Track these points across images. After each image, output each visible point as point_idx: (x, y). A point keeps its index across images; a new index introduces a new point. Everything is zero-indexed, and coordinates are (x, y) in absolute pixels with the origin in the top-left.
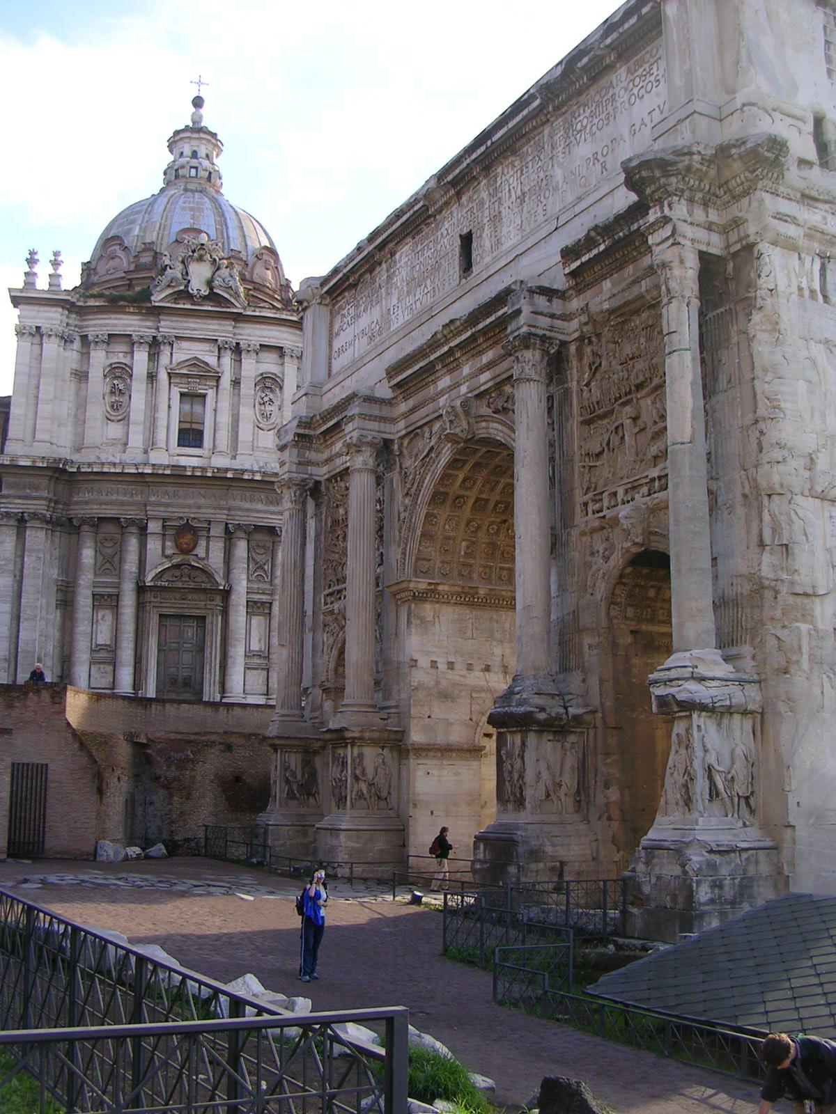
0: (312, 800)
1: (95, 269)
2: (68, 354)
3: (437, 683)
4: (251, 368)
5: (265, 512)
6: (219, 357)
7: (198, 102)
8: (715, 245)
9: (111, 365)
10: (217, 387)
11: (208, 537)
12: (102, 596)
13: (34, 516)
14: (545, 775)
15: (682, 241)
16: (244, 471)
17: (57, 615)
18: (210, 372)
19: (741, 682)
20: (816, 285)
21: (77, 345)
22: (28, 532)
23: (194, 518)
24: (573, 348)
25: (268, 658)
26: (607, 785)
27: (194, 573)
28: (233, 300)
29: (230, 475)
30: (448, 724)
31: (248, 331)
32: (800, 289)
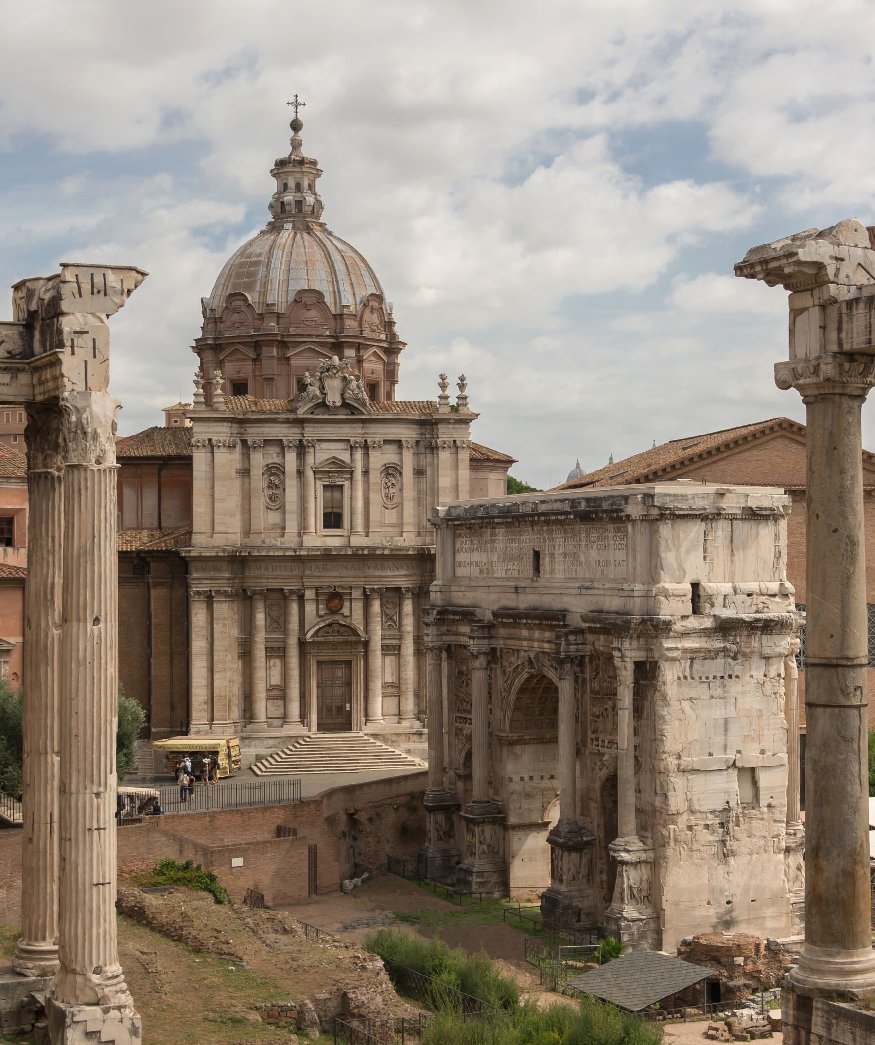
0: (452, 840)
1: (220, 318)
2: (233, 457)
3: (524, 788)
4: (378, 460)
5: (393, 577)
6: (351, 454)
7: (296, 126)
8: (640, 656)
9: (268, 465)
10: (352, 478)
11: (351, 600)
12: (273, 648)
13: (219, 593)
14: (572, 869)
15: (626, 659)
16: (375, 549)
17: (238, 665)
18: (345, 467)
19: (645, 850)
20: (688, 674)
21: (239, 448)
22: (215, 605)
23: (339, 586)
24: (587, 660)
25: (398, 687)
26: (601, 873)
27: (342, 629)
28: (361, 408)
29: (366, 552)
30: (530, 811)
31: (373, 430)
32: (679, 678)
